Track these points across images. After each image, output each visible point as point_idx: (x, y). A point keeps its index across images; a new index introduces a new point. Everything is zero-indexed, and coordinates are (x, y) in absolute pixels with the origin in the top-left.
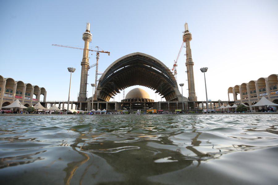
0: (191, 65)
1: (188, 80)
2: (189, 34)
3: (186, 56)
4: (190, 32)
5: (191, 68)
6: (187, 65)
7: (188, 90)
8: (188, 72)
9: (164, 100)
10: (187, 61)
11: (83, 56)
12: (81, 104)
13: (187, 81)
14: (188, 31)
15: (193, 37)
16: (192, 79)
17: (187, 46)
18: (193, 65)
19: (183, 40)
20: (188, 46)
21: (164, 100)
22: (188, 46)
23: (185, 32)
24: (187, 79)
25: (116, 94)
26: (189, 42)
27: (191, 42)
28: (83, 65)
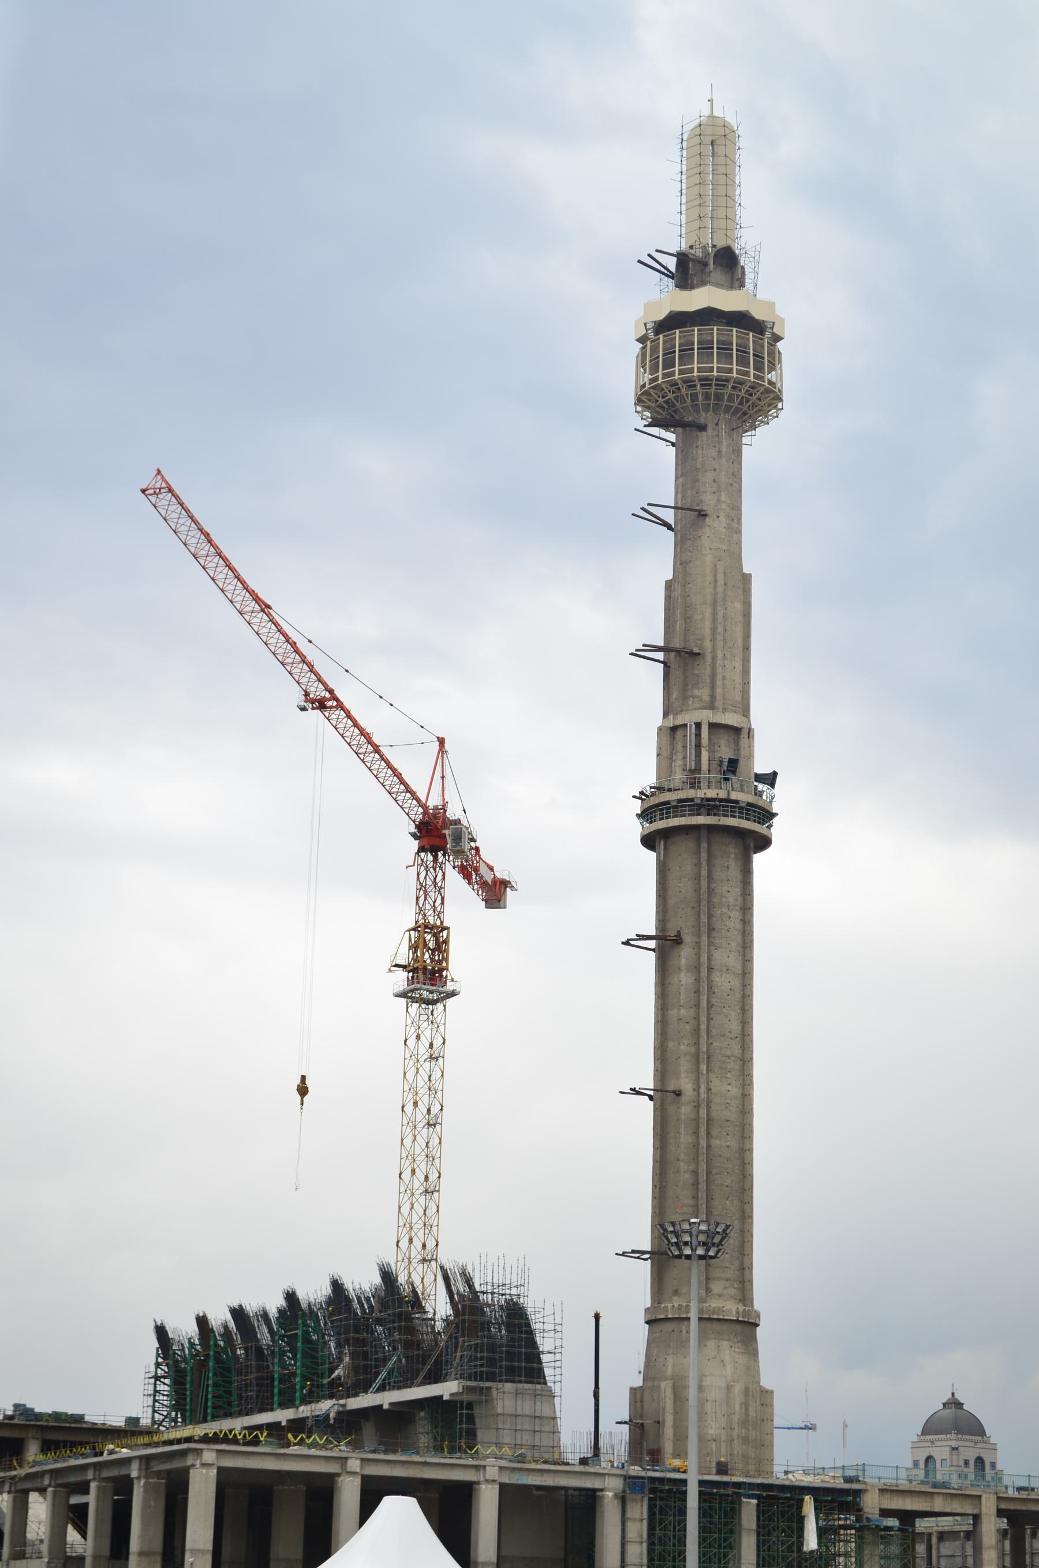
0: (732, 849)
1: (664, 1095)
2: (742, 320)
3: (651, 677)
4: (770, 286)
5: (728, 891)
6: (666, 834)
7: (644, 1268)
8: (666, 943)
10: (665, 759)
13: (646, 1108)
14: (727, 263)
16: (717, 1085)
18: (764, 843)
19: (643, 399)
20: (700, 519)
22: (700, 519)
23: (687, 270)
24: (647, 1080)
26: (738, 452)
27: (764, 450)
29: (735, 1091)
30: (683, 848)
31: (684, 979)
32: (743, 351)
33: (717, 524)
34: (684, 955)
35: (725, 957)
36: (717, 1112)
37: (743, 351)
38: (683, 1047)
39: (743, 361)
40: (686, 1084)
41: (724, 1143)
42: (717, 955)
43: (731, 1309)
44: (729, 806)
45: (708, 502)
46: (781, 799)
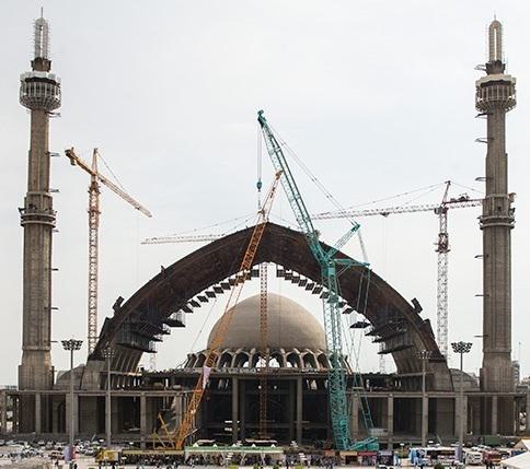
0: (502, 231)
1: (486, 296)
2: (501, 82)
4: (511, 71)
5: (501, 243)
8: (486, 256)
9: (389, 366)
11: (29, 183)
12: (38, 397)
15: (520, 95)
17: (490, 139)
19: (478, 106)
20: (495, 139)
21: (389, 366)
22: (495, 139)
25: (165, 333)
27: (511, 117)
28: (35, 231)
29: (502, 294)
30: (489, 230)
31: (489, 266)
32: (500, 91)
33: (497, 141)
34: (489, 260)
35: (500, 259)
36: (498, 299)
37: (506, 91)
38: (489, 283)
39: (501, 94)
40: (489, 293)
41: (500, 307)
42: (498, 260)
43: (502, 349)
44: (500, 220)
45: (494, 135)
46: (516, 215)
